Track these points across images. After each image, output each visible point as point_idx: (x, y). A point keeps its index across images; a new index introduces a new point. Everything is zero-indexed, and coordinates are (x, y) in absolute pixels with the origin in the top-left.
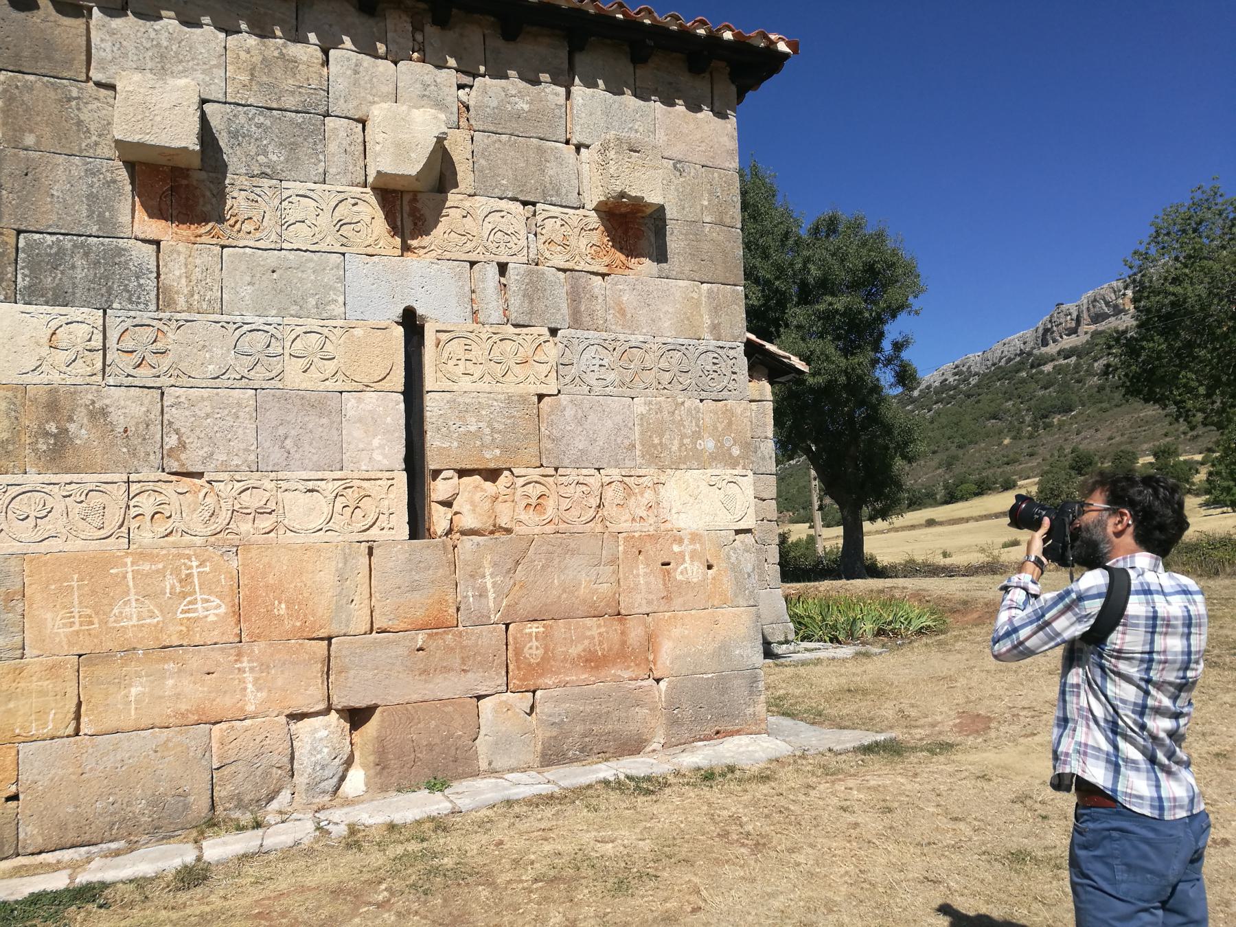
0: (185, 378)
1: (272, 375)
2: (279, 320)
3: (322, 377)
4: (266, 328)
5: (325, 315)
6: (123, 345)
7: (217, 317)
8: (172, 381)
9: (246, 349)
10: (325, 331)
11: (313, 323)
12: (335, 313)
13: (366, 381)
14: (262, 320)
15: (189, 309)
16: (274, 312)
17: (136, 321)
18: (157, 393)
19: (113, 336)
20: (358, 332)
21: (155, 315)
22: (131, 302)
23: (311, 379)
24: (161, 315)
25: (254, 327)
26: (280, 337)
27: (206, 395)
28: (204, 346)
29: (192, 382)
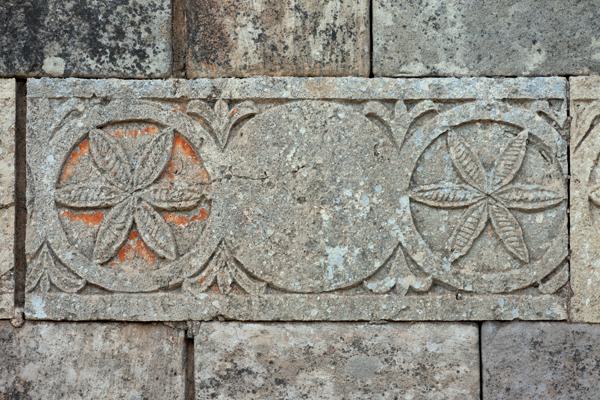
0: (256, 292)
1: (534, 273)
2: (553, 86)
4: (513, 114)
6: (71, 193)
7: (357, 85)
8: (218, 303)
9: (448, 187)
15: (272, 60)
16: (535, 59)
17: (114, 111)
18: (170, 346)
19: (45, 166)
21: (164, 87)
22: (96, 50)
24: (185, 87)
25: (471, 112)
26: (554, 139)
27: (320, 347)
28: (317, 186)
29: (280, 304)
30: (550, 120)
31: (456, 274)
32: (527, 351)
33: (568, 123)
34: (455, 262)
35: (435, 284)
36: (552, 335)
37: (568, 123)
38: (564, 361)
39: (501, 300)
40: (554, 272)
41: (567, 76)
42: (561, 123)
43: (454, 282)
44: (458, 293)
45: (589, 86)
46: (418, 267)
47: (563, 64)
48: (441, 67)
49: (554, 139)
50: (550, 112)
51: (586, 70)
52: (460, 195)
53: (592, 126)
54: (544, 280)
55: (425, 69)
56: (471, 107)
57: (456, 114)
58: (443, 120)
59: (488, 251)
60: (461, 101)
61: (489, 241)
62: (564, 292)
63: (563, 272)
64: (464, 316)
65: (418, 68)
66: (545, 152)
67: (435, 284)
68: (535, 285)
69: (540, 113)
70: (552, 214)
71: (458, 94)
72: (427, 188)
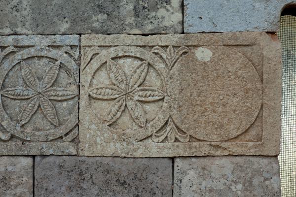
1: (61, 132)
2: (73, 39)
3: (142, 133)
4: (53, 53)
5: (149, 28)
9: (20, 89)
10: (148, 56)
11: (128, 41)
12: (167, 23)
13: (214, 138)
14: (46, 41)
16: (65, 26)
20: (203, 54)
23: (123, 138)
25: (33, 52)
26: (72, 65)
30: (71, 56)
31: (22, 132)
32: (56, 170)
33: (80, 57)
34: (22, 126)
35: (12, 137)
36: (69, 162)
37: (80, 57)
38: (75, 175)
39: (44, 145)
40: (71, 131)
41: (80, 35)
42: (76, 57)
43: (21, 136)
44: (23, 141)
45: (90, 39)
46: (4, 129)
47: (78, 29)
48: (19, 30)
49: (72, 65)
50: (71, 52)
51: (90, 31)
52: (26, 93)
53: (91, 59)
54: (66, 135)
55: (11, 31)
56: (33, 50)
57: (25, 53)
58: (19, 56)
59: (39, 120)
60: (28, 47)
61: (39, 115)
62: (75, 141)
63: (75, 131)
64: (26, 153)
65: (8, 31)
66: (68, 72)
67: (12, 137)
68: (61, 138)
69: (66, 53)
70: (71, 102)
71: (26, 43)
72: (10, 89)
